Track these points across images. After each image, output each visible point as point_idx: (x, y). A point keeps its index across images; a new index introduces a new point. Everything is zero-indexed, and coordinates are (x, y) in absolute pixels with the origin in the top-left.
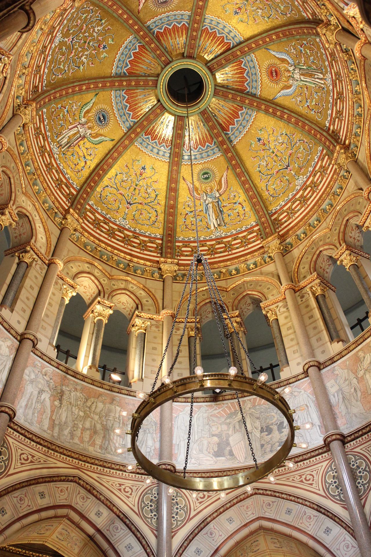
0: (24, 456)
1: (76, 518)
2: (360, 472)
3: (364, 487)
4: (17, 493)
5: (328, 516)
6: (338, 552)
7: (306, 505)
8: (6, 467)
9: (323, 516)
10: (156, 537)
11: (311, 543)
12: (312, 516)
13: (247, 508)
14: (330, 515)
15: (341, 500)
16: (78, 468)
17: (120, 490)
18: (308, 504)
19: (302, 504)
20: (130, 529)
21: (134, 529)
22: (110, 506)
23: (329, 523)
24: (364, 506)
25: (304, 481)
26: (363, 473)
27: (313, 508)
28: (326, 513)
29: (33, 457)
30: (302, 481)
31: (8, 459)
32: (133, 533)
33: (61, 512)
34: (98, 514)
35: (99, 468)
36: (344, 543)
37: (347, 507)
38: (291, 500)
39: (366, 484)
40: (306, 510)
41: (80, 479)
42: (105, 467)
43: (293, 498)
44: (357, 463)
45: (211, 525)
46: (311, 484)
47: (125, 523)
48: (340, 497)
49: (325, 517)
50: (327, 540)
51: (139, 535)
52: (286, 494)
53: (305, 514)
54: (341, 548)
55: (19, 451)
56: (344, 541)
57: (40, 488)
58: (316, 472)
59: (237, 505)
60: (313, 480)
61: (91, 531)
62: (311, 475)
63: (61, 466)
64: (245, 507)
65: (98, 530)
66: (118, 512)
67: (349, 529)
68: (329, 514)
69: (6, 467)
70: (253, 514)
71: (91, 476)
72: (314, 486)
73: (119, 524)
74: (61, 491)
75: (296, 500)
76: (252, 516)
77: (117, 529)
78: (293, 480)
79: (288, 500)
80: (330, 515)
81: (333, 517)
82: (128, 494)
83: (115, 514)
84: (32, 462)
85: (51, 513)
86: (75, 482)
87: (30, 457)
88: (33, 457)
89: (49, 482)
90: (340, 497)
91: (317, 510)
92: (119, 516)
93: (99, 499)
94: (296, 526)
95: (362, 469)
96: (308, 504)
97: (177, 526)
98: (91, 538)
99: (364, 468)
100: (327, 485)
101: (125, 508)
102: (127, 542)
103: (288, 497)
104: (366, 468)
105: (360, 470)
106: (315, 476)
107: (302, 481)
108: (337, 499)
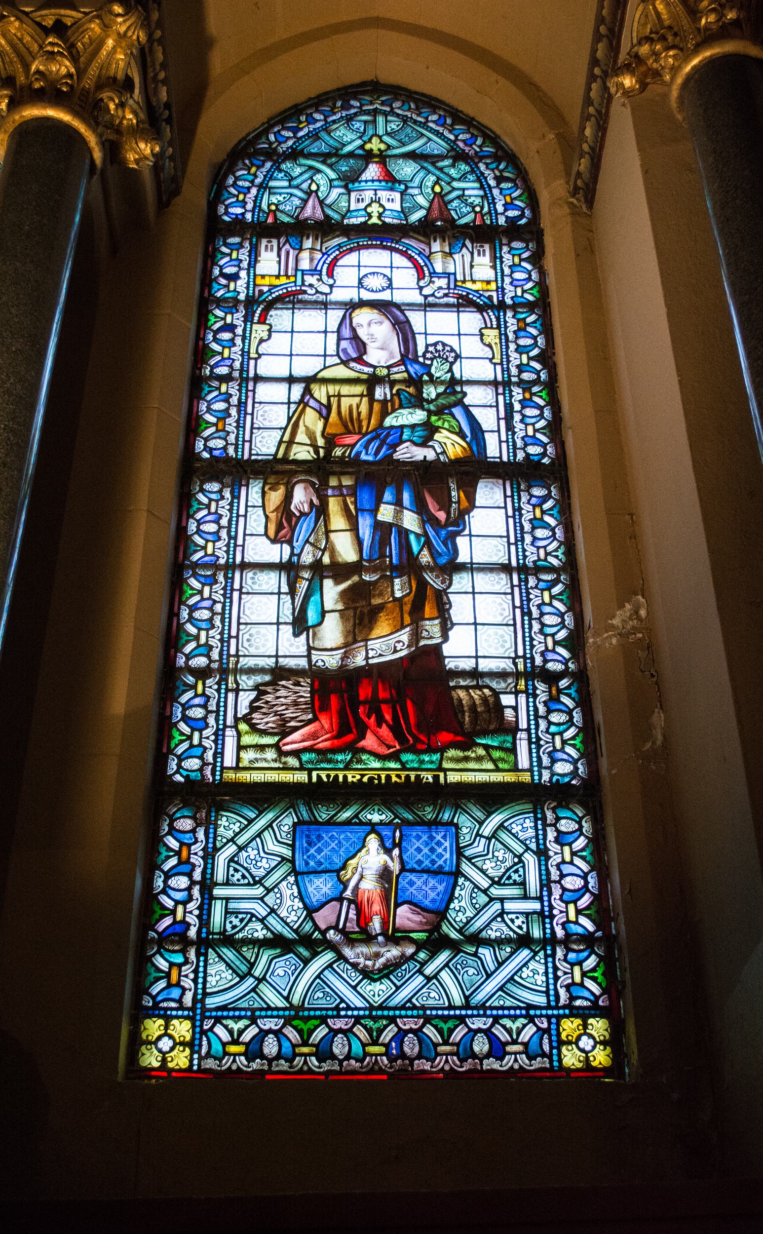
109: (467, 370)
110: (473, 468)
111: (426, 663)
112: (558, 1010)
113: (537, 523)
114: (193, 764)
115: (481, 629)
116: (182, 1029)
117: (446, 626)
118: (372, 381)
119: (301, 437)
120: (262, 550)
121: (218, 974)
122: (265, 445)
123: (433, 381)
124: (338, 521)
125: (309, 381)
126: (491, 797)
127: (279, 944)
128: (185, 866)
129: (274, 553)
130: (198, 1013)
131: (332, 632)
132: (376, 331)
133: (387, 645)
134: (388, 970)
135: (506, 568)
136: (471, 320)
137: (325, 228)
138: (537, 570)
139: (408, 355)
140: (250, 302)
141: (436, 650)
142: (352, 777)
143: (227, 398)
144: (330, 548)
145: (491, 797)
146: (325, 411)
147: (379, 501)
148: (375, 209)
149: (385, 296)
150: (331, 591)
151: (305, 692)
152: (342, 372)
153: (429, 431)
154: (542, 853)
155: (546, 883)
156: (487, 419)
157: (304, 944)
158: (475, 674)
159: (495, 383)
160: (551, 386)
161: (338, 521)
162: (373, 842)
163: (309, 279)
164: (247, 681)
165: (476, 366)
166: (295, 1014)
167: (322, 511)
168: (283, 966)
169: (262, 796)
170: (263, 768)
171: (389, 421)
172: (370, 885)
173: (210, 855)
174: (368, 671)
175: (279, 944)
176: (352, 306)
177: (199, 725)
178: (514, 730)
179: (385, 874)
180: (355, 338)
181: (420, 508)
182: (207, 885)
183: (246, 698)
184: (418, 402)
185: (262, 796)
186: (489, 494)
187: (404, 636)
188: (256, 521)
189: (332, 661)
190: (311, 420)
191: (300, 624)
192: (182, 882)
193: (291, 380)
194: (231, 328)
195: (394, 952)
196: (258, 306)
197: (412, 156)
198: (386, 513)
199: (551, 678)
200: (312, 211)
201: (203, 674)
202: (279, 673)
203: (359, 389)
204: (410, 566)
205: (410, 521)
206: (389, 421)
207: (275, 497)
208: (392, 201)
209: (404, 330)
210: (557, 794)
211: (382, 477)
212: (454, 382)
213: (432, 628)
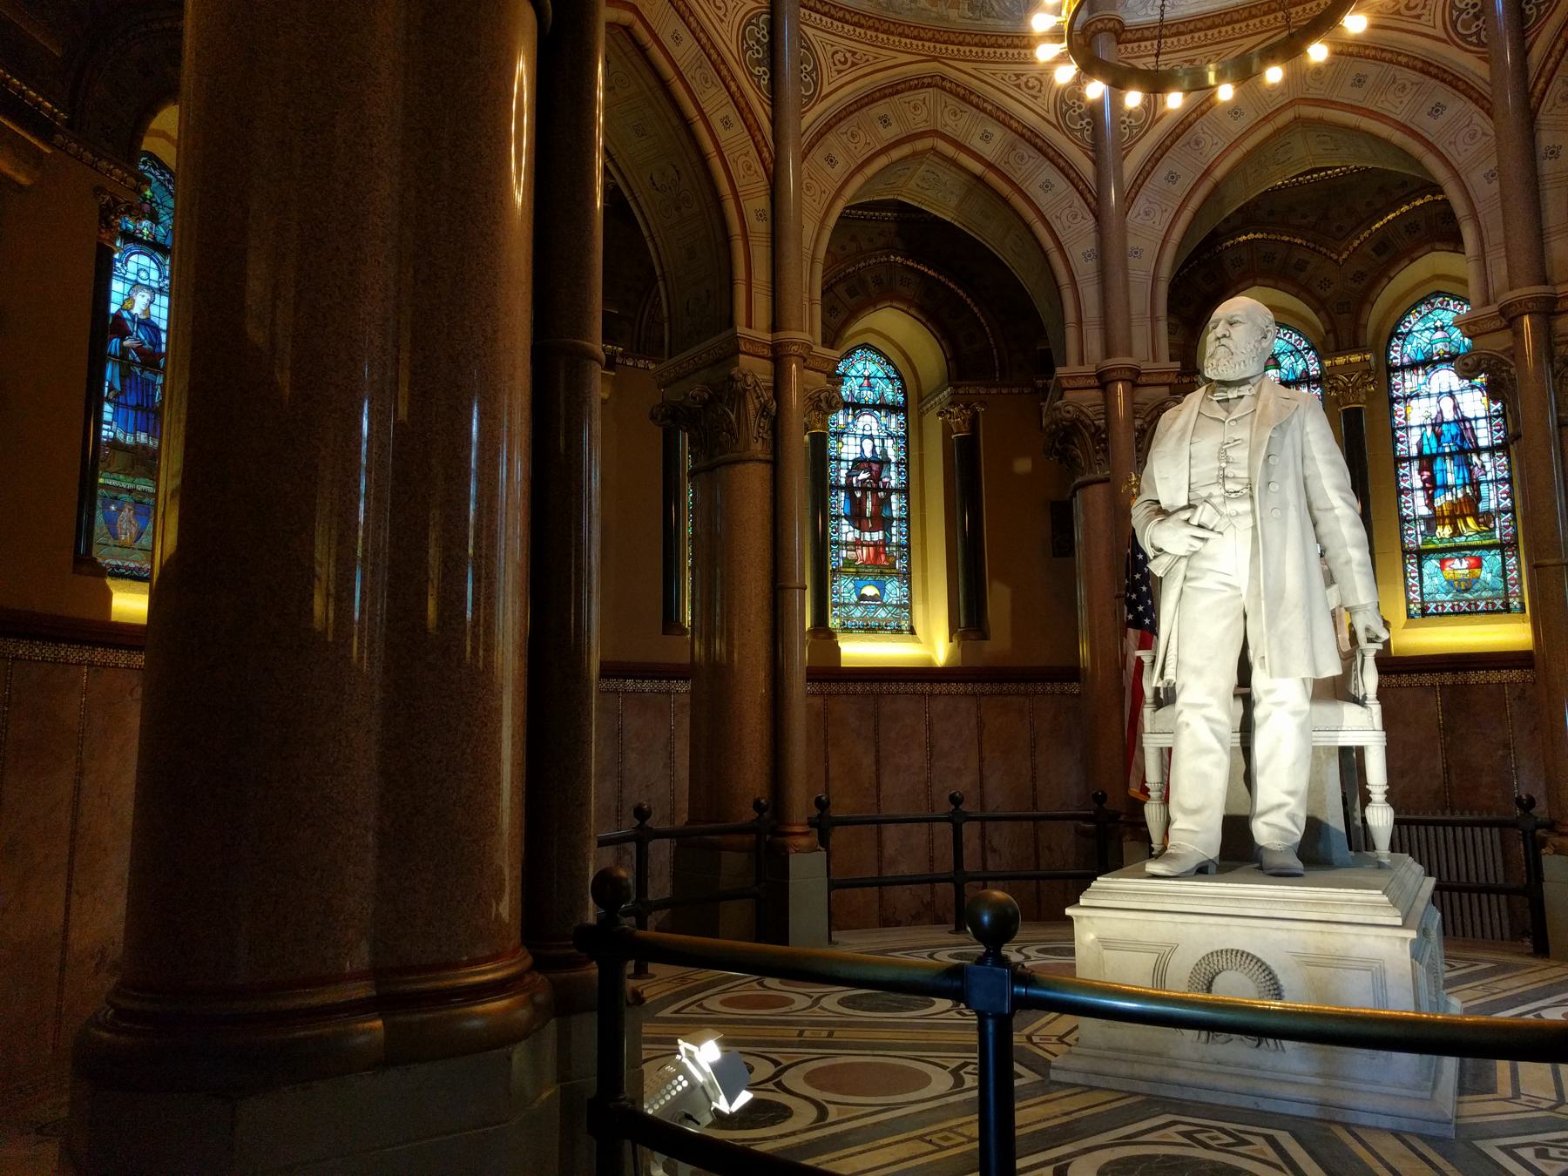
0: (839, 56)
1: (950, 150)
3: (1539, 10)
4: (843, 127)
5: (1443, 81)
7: (1399, 64)
8: (816, 84)
10: (1094, 163)
11: (1397, 137)
12: (1408, 85)
15: (1480, 44)
16: (935, 59)
17: (1018, 86)
19: (1391, 62)
20: (1046, 155)
21: (1052, 153)
22: (1003, 118)
23: (1442, 93)
24: (1527, 53)
25: (1403, 11)
27: (1414, 68)
29: (854, 54)
31: (815, 68)
32: (1052, 161)
33: (920, 145)
34: (986, 137)
35: (974, 49)
37: (1488, 55)
41: (943, 79)
42: (984, 45)
45: (1197, 126)
46: (1418, 17)
47: (1035, 146)
48: (1479, 38)
50: (1430, 127)
51: (1063, 164)
55: (828, 48)
57: (880, 108)
61: (977, 168)
63: (902, 60)
65: (989, 165)
66: (1020, 129)
69: (816, 84)
71: (962, 71)
73: (1025, 150)
74: (915, 108)
77: (1022, 158)
82: (1033, 92)
83: (1016, 132)
84: (854, 64)
85: (906, 150)
86: (936, 86)
87: (848, 55)
88: (854, 54)
89: (891, 95)
90: (1479, 38)
91: (1422, 71)
92: (1022, 136)
93: (984, 110)
97: (1131, 137)
98: (979, 179)
100: (1455, 14)
101: (1031, 119)
102: (1042, 178)
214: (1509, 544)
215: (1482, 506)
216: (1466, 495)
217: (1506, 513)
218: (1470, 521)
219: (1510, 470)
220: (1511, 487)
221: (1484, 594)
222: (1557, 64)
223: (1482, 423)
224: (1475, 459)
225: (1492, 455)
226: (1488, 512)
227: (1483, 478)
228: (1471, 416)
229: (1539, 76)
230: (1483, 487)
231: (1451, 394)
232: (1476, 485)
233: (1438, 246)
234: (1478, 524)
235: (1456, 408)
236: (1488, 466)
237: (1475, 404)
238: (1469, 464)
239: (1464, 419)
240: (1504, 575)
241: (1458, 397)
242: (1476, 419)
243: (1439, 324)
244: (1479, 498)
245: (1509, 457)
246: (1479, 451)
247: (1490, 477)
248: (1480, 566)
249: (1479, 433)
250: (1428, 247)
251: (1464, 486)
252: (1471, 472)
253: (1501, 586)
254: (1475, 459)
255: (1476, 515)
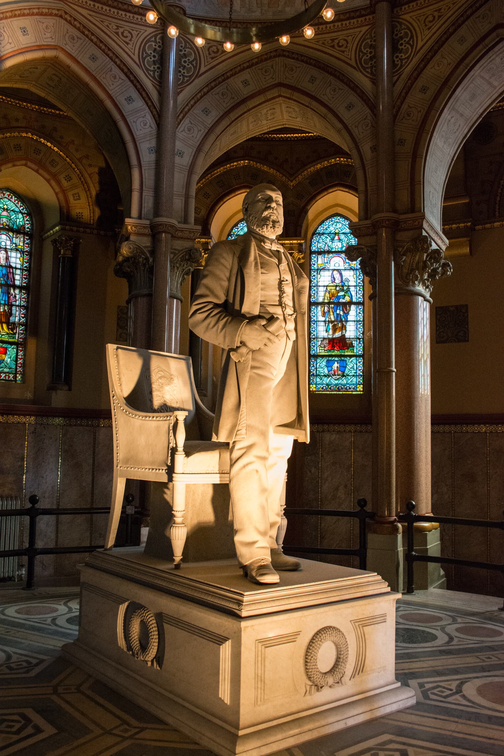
2: (185, 62)
5: (136, 86)
6: (134, 124)
7: (115, 63)
9: (129, 83)
13: (47, 27)
14: (139, 87)
18: (119, 62)
19: (111, 58)
23: (134, 94)
26: (188, 65)
27: (122, 70)
28: (135, 82)
30: (117, 33)
36: (141, 119)
38: (100, 48)
39: (187, 77)
40: (113, 67)
43: (103, 47)
44: (185, 51)
49: (131, 85)
50: (127, 108)
52: (97, 38)
53: (111, 71)
54: (138, 122)
56: (143, 117)
58: (136, 33)
59: (35, 17)
60: (131, 40)
62: (130, 32)
64: (45, 25)
67: (154, 110)
68: (137, 84)
70: (53, 39)
72: (130, 46)
75: (106, 50)
76: (50, 40)
78: (107, 26)
79: (96, 45)
80: (139, 87)
81: (141, 90)
94: (97, 77)
95: (189, 60)
96: (119, 62)
99: (191, 60)
103: (98, 43)
104: (193, 61)
105: (186, 60)
106: (134, 36)
107: (117, 33)
108: (150, 75)
109: (350, 284)
110: (351, 303)
111: (343, 336)
112: (357, 384)
113: (359, 313)
114: (313, 352)
115: (351, 331)
116: (314, 386)
117: (346, 331)
118: (336, 286)
119: (326, 298)
120: (321, 318)
121: (318, 380)
122: (321, 300)
123: (346, 286)
124: (331, 313)
125: (327, 286)
126: (351, 356)
127: (325, 376)
128: (314, 366)
129: (323, 319)
130: (316, 384)
131: (331, 332)
132: (336, 275)
133: (338, 334)
134: (338, 379)
135: (355, 321)
136: (352, 273)
137: (329, 252)
138: (359, 321)
139: (342, 281)
140: (317, 270)
141: (344, 335)
142: (333, 354)
143: (315, 290)
144: (330, 318)
145: (351, 356)
146: (329, 292)
147: (337, 309)
148: (337, 247)
149: (338, 268)
150: (331, 325)
151: (327, 342)
152: (332, 284)
153: (345, 296)
154: (357, 364)
155: (357, 368)
156: (353, 294)
157: (328, 376)
158: (349, 338)
159: (355, 286)
160: (363, 286)
161: (331, 313)
162: (336, 363)
163: (327, 265)
164: (320, 340)
165: (352, 283)
166: (327, 385)
167: (329, 311)
168: (325, 379)
169: (323, 356)
170: (323, 354)
171: (339, 294)
172: (336, 368)
173: (316, 365)
174: (335, 338)
175: (325, 376)
176: (334, 270)
177: (314, 346)
178: (354, 347)
179: (337, 367)
180: (334, 277)
181: (343, 311)
182: (316, 368)
183: (320, 342)
184: (343, 290)
185: (323, 356)
186: (353, 307)
187: (340, 333)
188: (320, 314)
189: (330, 337)
190: (327, 295)
191: (327, 331)
192: (313, 368)
193: (324, 286)
194: (314, 276)
195: (338, 377)
196: (319, 270)
197: (343, 233)
198: (338, 312)
199: (359, 339)
200: (326, 248)
201: (314, 339)
202: (324, 339)
203: (334, 288)
204: (341, 321)
205: (342, 313)
206: (339, 294)
207: (323, 309)
208: (340, 245)
209: (341, 275)
210: (359, 356)
211: (338, 304)
212: (349, 286)
213: (344, 331)
214: (21, 344)
215: (12, 319)
216: (5, 310)
217: (23, 326)
218: (5, 326)
219: (28, 302)
220: (27, 312)
221: (6, 370)
222: (189, 110)
223: (18, 272)
224: (12, 291)
225: (20, 292)
226: (14, 323)
227: (14, 303)
228: (13, 265)
229: (181, 112)
230: (14, 308)
231: (6, 250)
232: (10, 306)
233: (29, 164)
234: (8, 329)
235: (7, 258)
236: (18, 297)
237: (16, 260)
238: (9, 293)
239: (11, 267)
240: (16, 361)
241: (9, 253)
242: (16, 268)
243: (5, 207)
244: (11, 314)
245: (28, 295)
246: (15, 287)
247: (17, 303)
248: (5, 353)
249: (17, 277)
250: (24, 162)
251: (5, 305)
252: (9, 298)
253: (14, 367)
254: (12, 291)
255: (8, 323)
